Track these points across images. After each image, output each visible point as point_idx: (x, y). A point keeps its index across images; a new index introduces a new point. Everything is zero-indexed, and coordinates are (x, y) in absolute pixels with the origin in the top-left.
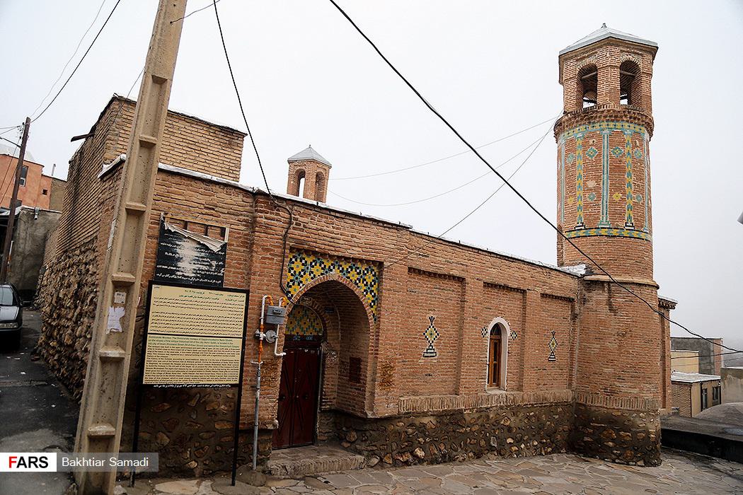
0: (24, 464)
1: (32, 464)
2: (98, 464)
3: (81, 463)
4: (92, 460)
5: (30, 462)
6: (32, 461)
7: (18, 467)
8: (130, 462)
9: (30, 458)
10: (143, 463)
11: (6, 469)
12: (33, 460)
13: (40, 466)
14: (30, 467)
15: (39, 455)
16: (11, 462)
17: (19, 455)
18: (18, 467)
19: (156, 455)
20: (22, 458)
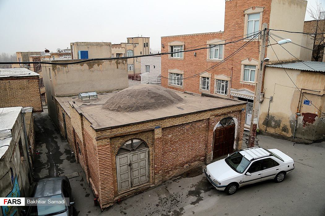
0: (11, 202)
1: (14, 203)
2: (43, 203)
3: (36, 202)
4: (40, 201)
5: (13, 202)
6: (14, 201)
7: (8, 204)
9: (13, 200)
10: (62, 202)
11: (2, 205)
12: (14, 201)
13: (18, 203)
14: (13, 204)
15: (17, 199)
16: (5, 202)
17: (8, 198)
18: (8, 204)
20: (10, 200)
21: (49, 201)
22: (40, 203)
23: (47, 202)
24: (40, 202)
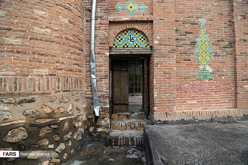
0: (8, 155)
1: (11, 155)
3: (27, 154)
5: (10, 154)
6: (11, 154)
7: (6, 156)
9: (10, 153)
11: (2, 156)
12: (11, 153)
13: (13, 155)
14: (10, 156)
15: (13, 152)
16: (4, 154)
17: (6, 152)
18: (6, 156)
20: (7, 153)
22: (31, 155)
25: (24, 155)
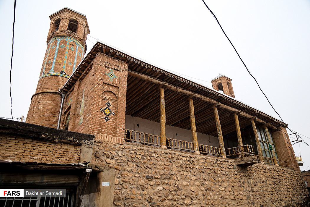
0: (10, 194)
1: (13, 194)
2: (41, 194)
3: (34, 194)
4: (38, 192)
5: (13, 193)
7: (7, 195)
8: (54, 193)
9: (12, 191)
10: (60, 194)
12: (14, 192)
13: (17, 195)
14: (12, 195)
15: (16, 190)
16: (4, 193)
17: (8, 190)
18: (7, 195)
19: (65, 190)
20: (9, 192)
21: (47, 192)
22: (38, 194)
23: (45, 194)
24: (38, 193)
25: (30, 194)
